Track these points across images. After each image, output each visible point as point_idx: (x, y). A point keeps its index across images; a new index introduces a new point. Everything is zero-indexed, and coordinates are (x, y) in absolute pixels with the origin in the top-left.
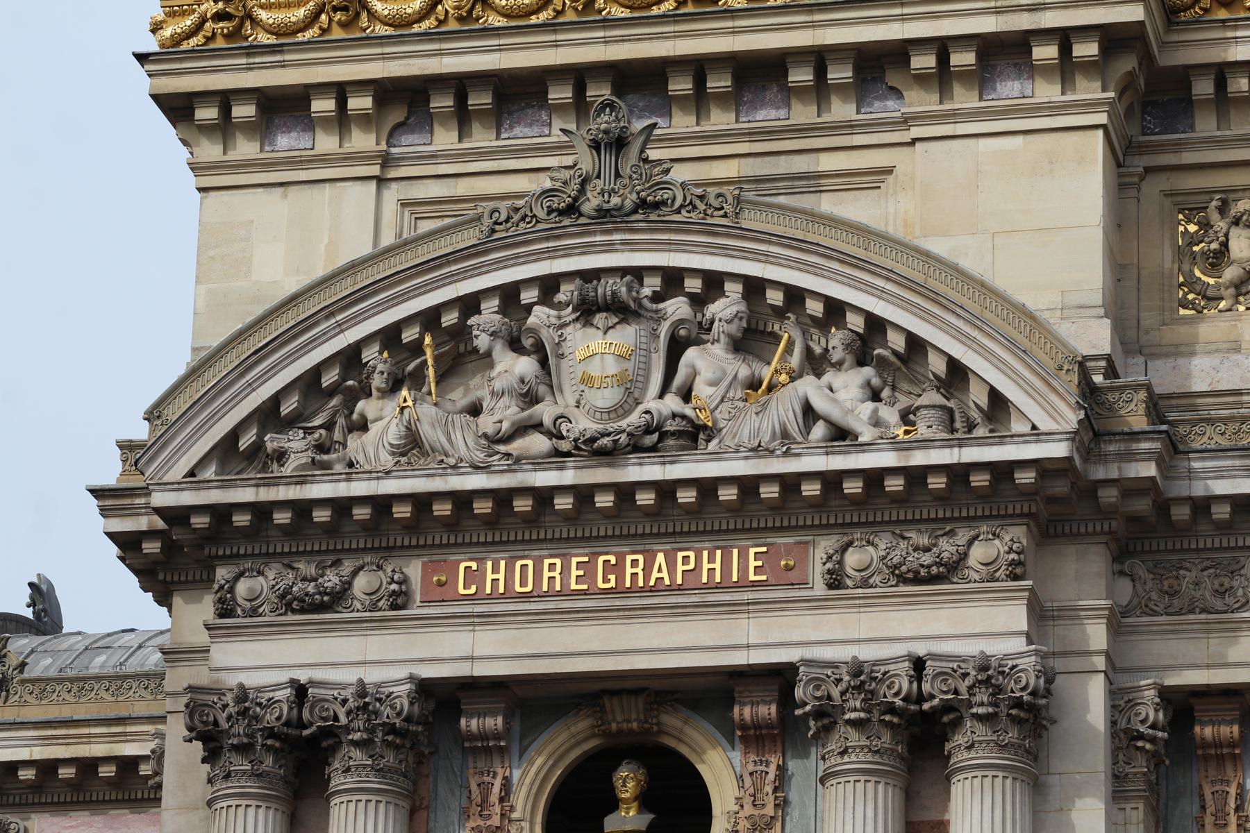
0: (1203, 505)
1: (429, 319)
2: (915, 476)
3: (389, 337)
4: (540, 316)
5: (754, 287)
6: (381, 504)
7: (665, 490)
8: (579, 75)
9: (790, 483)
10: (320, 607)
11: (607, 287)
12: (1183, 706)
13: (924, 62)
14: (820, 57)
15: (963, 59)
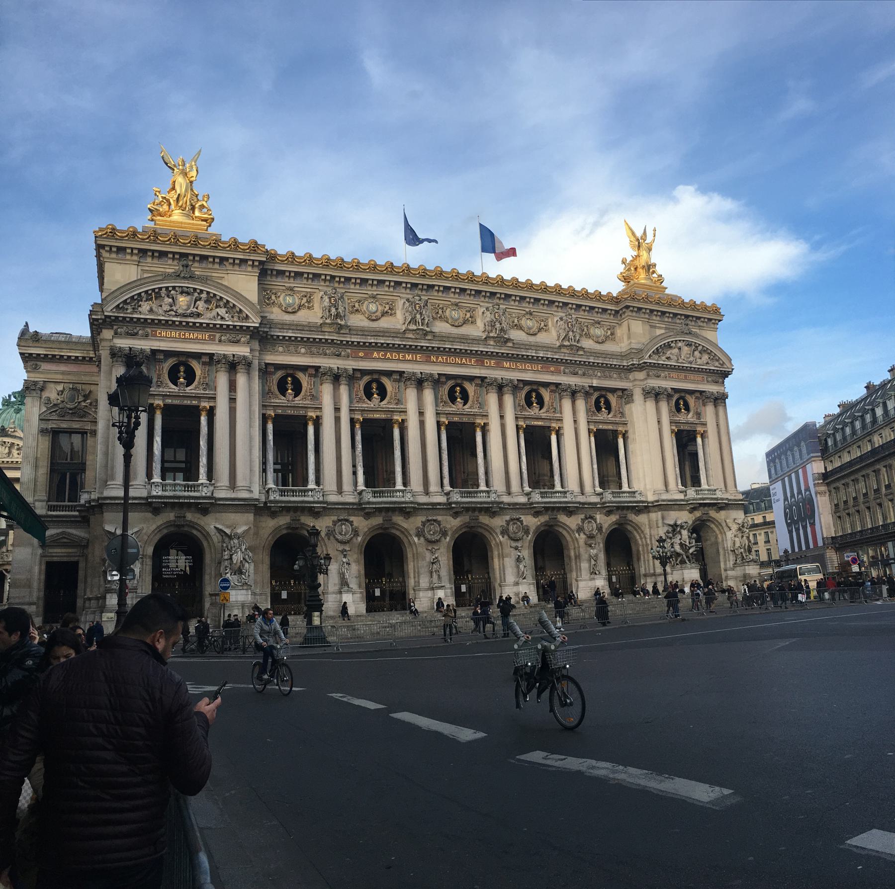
0: (272, 336)
1: (153, 290)
2: (235, 326)
3: (146, 292)
4: (173, 292)
5: (208, 293)
6: (146, 320)
7: (194, 323)
8: (174, 253)
9: (215, 325)
10: (134, 335)
11: (186, 289)
12: (267, 364)
13: (231, 261)
14: (214, 257)
15: (237, 262)
